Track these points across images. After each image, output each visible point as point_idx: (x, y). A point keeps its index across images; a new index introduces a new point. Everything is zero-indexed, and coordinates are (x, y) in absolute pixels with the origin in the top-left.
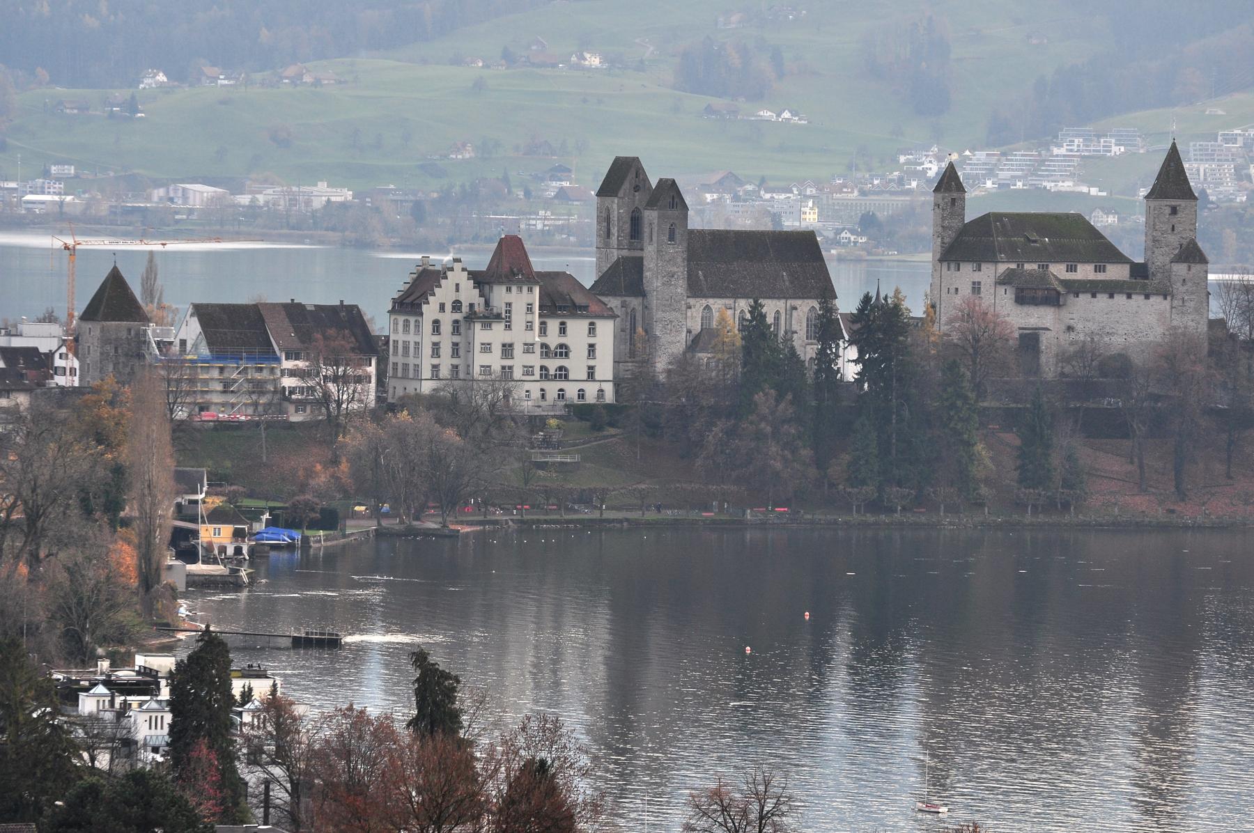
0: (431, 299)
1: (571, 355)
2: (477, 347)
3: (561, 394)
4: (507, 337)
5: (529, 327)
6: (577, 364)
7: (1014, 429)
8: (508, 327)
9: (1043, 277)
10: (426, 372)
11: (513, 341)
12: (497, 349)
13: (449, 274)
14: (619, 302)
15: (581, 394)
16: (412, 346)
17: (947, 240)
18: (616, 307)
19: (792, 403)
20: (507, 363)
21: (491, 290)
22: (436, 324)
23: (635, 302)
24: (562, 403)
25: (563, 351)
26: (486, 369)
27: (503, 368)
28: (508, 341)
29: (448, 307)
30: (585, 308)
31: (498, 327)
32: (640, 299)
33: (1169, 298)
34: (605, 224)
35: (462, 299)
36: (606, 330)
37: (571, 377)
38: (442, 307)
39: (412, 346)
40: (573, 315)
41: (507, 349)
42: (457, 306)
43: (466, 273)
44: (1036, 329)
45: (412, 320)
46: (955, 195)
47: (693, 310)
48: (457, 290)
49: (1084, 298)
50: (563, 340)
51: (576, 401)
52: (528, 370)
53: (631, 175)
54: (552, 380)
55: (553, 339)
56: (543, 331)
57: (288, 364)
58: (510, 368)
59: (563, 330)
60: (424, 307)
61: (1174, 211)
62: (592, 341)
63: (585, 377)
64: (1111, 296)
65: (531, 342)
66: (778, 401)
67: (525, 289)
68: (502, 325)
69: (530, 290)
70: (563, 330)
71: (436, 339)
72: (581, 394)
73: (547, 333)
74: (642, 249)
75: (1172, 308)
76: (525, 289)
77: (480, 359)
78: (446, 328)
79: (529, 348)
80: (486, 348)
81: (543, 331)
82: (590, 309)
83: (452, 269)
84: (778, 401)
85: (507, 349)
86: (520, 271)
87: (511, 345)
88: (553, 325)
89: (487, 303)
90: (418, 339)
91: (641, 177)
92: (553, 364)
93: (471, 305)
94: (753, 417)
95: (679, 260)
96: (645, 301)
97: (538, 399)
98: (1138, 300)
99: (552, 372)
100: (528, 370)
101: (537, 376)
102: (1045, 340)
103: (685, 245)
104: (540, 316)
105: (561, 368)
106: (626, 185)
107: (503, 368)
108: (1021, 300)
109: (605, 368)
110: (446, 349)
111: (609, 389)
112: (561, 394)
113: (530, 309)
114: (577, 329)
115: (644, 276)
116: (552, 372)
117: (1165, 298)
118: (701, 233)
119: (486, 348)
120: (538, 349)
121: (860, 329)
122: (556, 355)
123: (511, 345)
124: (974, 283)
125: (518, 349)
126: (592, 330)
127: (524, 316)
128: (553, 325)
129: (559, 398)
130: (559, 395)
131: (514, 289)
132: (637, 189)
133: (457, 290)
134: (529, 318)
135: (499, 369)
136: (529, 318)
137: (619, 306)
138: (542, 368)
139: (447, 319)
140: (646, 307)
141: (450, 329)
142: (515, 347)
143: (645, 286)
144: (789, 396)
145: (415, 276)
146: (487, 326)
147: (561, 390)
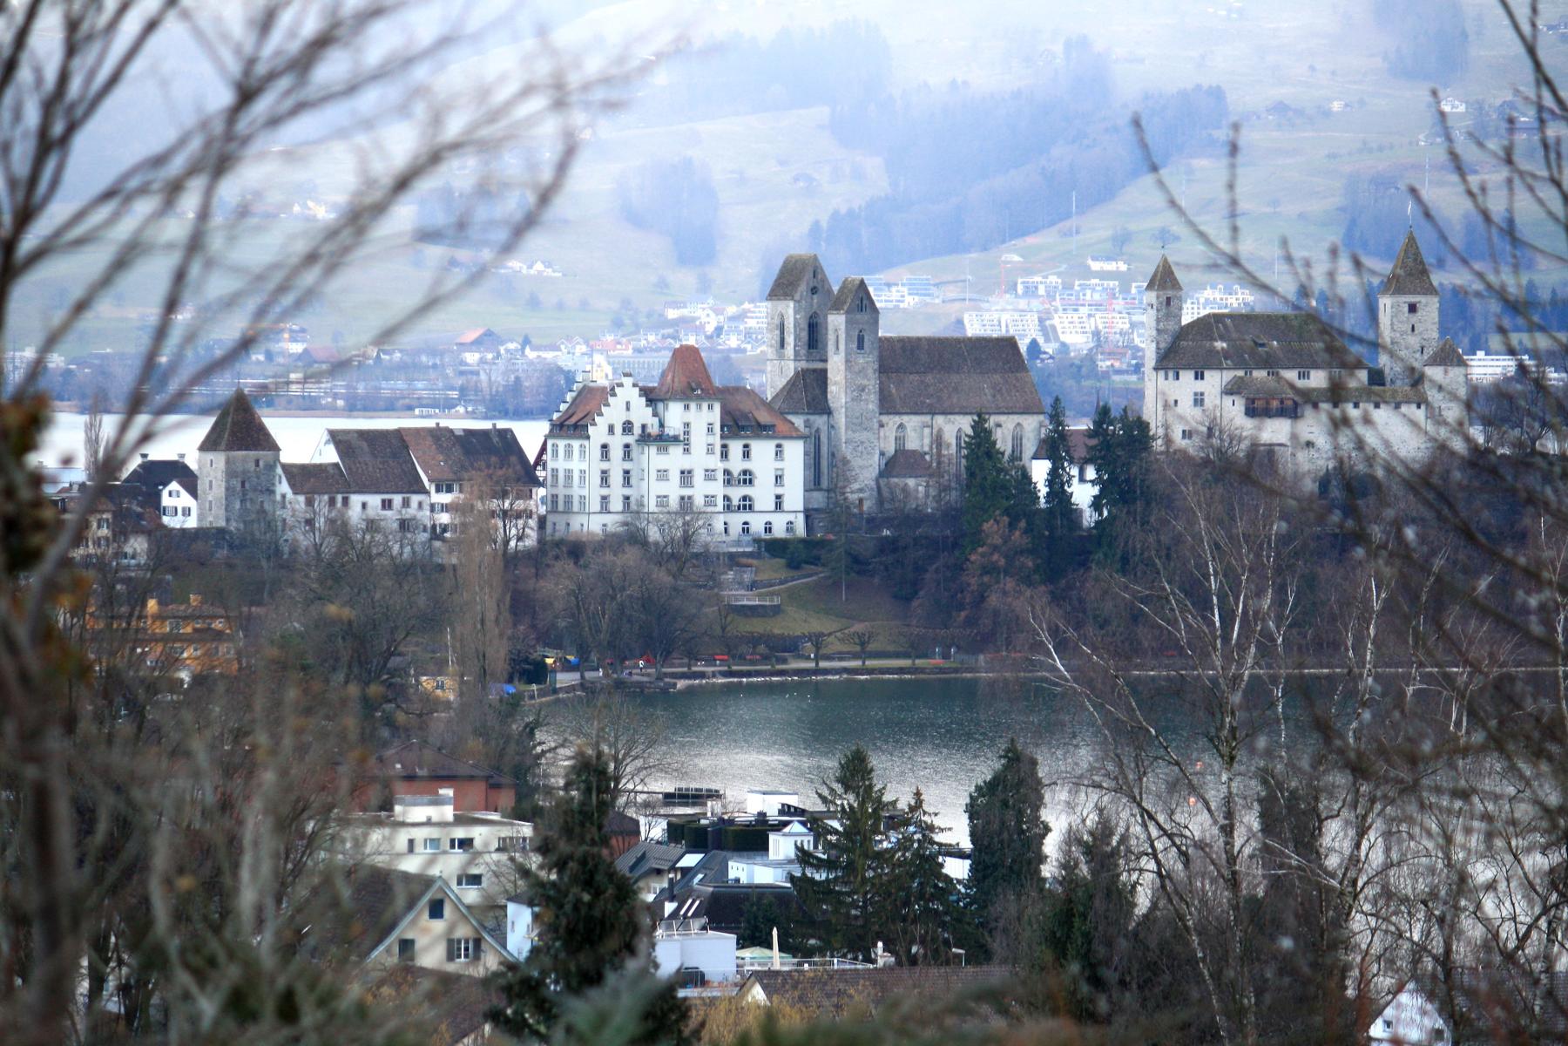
4: (686, 462)
5: (710, 451)
6: (762, 493)
12: (675, 477)
17: (1163, 345)
20: (686, 492)
24: (747, 538)
25: (747, 478)
28: (687, 467)
29: (618, 429)
38: (611, 429)
41: (686, 476)
46: (1170, 293)
48: (628, 409)
50: (747, 465)
51: (764, 536)
55: (736, 464)
59: (746, 455)
61: (1413, 308)
63: (772, 507)
70: (746, 455)
74: (825, 361)
85: (686, 476)
86: (699, 386)
92: (736, 493)
93: (644, 427)
99: (735, 502)
100: (710, 500)
101: (720, 508)
109: (795, 497)
114: (763, 450)
116: (735, 502)
118: (888, 340)
120: (720, 476)
124: (1196, 394)
128: (736, 447)
147: (746, 523)
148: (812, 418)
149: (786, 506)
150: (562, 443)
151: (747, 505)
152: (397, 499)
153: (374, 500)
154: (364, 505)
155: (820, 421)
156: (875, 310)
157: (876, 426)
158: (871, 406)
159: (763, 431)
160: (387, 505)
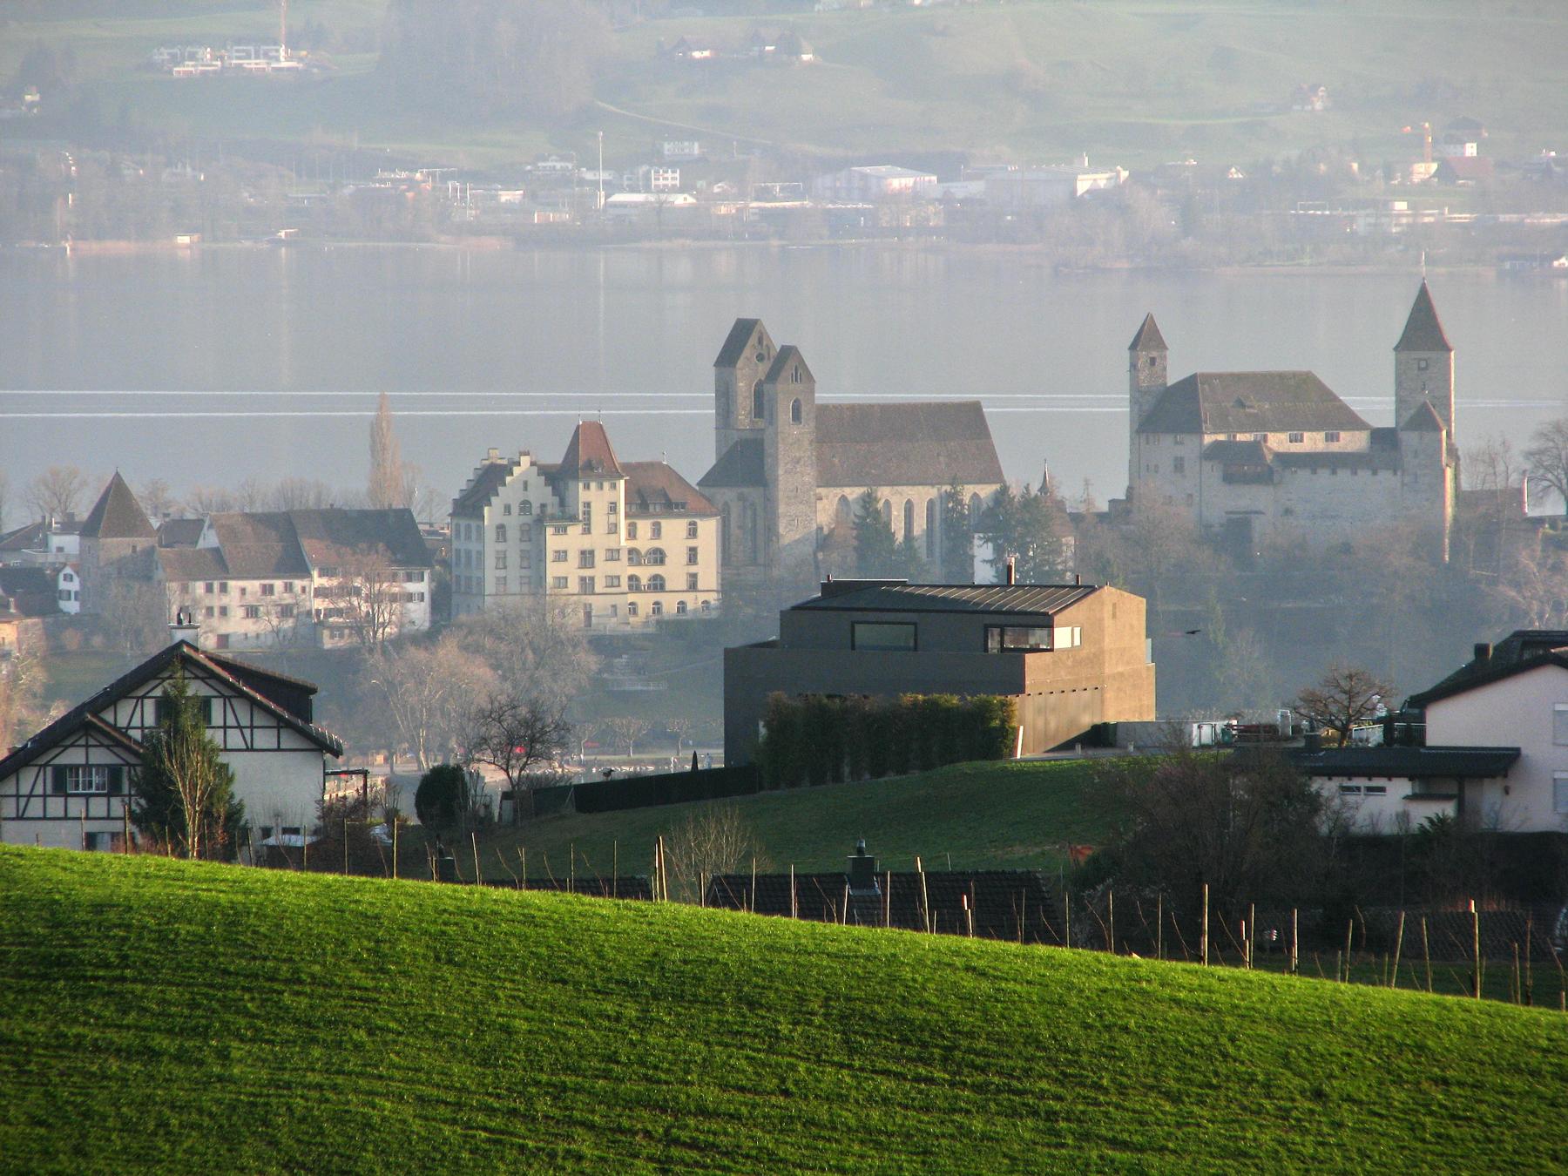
0: (494, 499)
2: (550, 556)
4: (586, 543)
5: (613, 530)
6: (676, 573)
8: (587, 531)
9: (1255, 449)
10: (490, 587)
12: (574, 559)
13: (517, 470)
20: (587, 573)
24: (656, 617)
25: (658, 557)
26: (562, 581)
27: (583, 579)
28: (587, 547)
29: (515, 510)
31: (575, 530)
33: (1399, 473)
35: (531, 499)
36: (709, 528)
37: (668, 587)
38: (508, 509)
39: (474, 555)
41: (587, 558)
42: (525, 506)
43: (535, 468)
44: (1246, 513)
45: (474, 524)
48: (526, 488)
49: (1303, 475)
50: (656, 544)
55: (644, 542)
56: (632, 534)
57: (318, 581)
58: (592, 579)
59: (657, 532)
62: (692, 543)
64: (1334, 472)
65: (615, 547)
67: (606, 485)
69: (614, 487)
70: (657, 532)
72: (682, 606)
75: (1403, 484)
77: (553, 570)
78: (513, 534)
79: (613, 555)
80: (561, 556)
83: (519, 464)
85: (587, 558)
87: (592, 552)
89: (562, 503)
92: (645, 573)
93: (543, 506)
98: (1364, 475)
99: (644, 581)
100: (613, 581)
102: (1259, 527)
104: (627, 516)
105: (656, 577)
107: (583, 579)
108: (1229, 479)
109: (709, 573)
110: (514, 559)
111: (713, 598)
113: (613, 508)
114: (674, 530)
116: (644, 581)
117: (1395, 473)
119: (561, 556)
120: (624, 556)
123: (592, 552)
125: (600, 556)
126: (693, 533)
127: (605, 517)
128: (644, 527)
131: (593, 485)
133: (526, 488)
134: (612, 518)
138: (631, 578)
139: (514, 522)
141: (518, 535)
146: (561, 530)
147: (656, 603)
148: (745, 490)
149: (700, 586)
150: (463, 522)
151: (658, 584)
152: (278, 584)
153: (254, 586)
154: (243, 591)
155: (753, 493)
156: (810, 379)
157: (813, 499)
158: (806, 479)
159: (671, 507)
160: (268, 590)
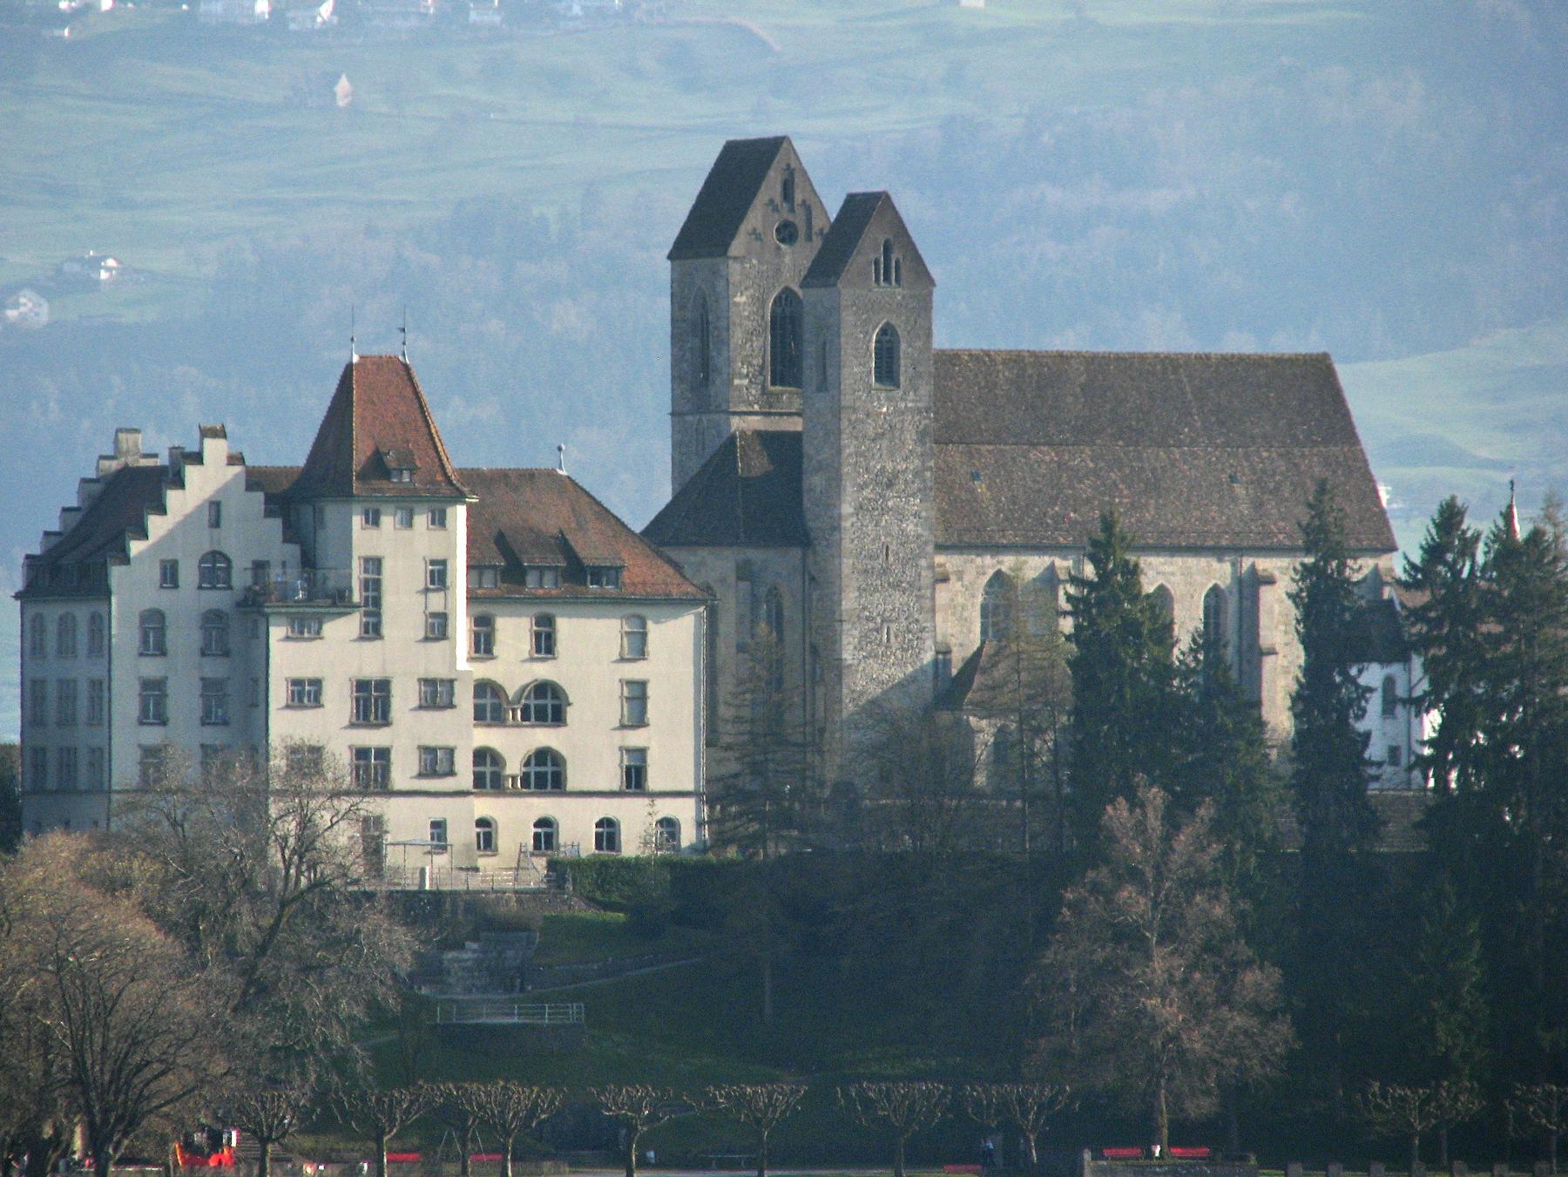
0: (136, 547)
1: (571, 714)
2: (278, 693)
3: (546, 832)
4: (370, 661)
7: (1347, 616)
11: (388, 674)
12: (338, 702)
13: (191, 472)
14: (731, 565)
15: (608, 832)
16: (83, 689)
18: (723, 581)
19: (1218, 828)
20: (372, 738)
21: (319, 521)
22: (154, 630)
23: (778, 563)
28: (372, 672)
29: (189, 574)
30: (611, 573)
31: (342, 629)
32: (796, 553)
34: (695, 342)
35: (231, 547)
37: (572, 783)
38: (170, 574)
40: (579, 602)
42: (215, 568)
45: (81, 612)
47: (954, 584)
48: (216, 523)
50: (543, 671)
52: (435, 762)
53: (771, 187)
54: (515, 794)
56: (483, 645)
58: (383, 754)
59: (545, 644)
60: (116, 573)
63: (614, 781)
66: (1172, 824)
67: (421, 520)
68: (350, 625)
69: (439, 520)
70: (545, 644)
71: (152, 668)
72: (608, 832)
73: (496, 651)
76: (421, 520)
79: (436, 695)
80: (306, 693)
81: (483, 645)
82: (626, 576)
83: (197, 458)
84: (1172, 824)
87: (384, 686)
88: (514, 631)
90: (98, 672)
91: (799, 197)
94: (1102, 874)
95: (910, 437)
96: (811, 559)
97: (467, 846)
99: (514, 767)
100: (435, 762)
103: (926, 389)
104: (472, 599)
106: (756, 218)
107: (361, 753)
110: (184, 701)
111: (685, 813)
112: (546, 832)
113: (438, 576)
115: (805, 485)
116: (514, 767)
119: (306, 693)
121: (1426, 608)
122: (525, 717)
125: (404, 698)
126: (638, 648)
129: (537, 846)
130: (537, 837)
131: (387, 521)
132: (787, 233)
133: (216, 523)
135: (345, 758)
136: (436, 602)
137: (732, 578)
138: (481, 755)
140: (813, 579)
141: (195, 638)
142: (396, 691)
143: (808, 516)
144: (1205, 812)
145: (97, 488)
146: (306, 626)
